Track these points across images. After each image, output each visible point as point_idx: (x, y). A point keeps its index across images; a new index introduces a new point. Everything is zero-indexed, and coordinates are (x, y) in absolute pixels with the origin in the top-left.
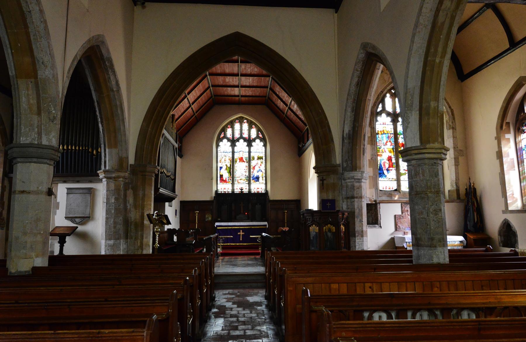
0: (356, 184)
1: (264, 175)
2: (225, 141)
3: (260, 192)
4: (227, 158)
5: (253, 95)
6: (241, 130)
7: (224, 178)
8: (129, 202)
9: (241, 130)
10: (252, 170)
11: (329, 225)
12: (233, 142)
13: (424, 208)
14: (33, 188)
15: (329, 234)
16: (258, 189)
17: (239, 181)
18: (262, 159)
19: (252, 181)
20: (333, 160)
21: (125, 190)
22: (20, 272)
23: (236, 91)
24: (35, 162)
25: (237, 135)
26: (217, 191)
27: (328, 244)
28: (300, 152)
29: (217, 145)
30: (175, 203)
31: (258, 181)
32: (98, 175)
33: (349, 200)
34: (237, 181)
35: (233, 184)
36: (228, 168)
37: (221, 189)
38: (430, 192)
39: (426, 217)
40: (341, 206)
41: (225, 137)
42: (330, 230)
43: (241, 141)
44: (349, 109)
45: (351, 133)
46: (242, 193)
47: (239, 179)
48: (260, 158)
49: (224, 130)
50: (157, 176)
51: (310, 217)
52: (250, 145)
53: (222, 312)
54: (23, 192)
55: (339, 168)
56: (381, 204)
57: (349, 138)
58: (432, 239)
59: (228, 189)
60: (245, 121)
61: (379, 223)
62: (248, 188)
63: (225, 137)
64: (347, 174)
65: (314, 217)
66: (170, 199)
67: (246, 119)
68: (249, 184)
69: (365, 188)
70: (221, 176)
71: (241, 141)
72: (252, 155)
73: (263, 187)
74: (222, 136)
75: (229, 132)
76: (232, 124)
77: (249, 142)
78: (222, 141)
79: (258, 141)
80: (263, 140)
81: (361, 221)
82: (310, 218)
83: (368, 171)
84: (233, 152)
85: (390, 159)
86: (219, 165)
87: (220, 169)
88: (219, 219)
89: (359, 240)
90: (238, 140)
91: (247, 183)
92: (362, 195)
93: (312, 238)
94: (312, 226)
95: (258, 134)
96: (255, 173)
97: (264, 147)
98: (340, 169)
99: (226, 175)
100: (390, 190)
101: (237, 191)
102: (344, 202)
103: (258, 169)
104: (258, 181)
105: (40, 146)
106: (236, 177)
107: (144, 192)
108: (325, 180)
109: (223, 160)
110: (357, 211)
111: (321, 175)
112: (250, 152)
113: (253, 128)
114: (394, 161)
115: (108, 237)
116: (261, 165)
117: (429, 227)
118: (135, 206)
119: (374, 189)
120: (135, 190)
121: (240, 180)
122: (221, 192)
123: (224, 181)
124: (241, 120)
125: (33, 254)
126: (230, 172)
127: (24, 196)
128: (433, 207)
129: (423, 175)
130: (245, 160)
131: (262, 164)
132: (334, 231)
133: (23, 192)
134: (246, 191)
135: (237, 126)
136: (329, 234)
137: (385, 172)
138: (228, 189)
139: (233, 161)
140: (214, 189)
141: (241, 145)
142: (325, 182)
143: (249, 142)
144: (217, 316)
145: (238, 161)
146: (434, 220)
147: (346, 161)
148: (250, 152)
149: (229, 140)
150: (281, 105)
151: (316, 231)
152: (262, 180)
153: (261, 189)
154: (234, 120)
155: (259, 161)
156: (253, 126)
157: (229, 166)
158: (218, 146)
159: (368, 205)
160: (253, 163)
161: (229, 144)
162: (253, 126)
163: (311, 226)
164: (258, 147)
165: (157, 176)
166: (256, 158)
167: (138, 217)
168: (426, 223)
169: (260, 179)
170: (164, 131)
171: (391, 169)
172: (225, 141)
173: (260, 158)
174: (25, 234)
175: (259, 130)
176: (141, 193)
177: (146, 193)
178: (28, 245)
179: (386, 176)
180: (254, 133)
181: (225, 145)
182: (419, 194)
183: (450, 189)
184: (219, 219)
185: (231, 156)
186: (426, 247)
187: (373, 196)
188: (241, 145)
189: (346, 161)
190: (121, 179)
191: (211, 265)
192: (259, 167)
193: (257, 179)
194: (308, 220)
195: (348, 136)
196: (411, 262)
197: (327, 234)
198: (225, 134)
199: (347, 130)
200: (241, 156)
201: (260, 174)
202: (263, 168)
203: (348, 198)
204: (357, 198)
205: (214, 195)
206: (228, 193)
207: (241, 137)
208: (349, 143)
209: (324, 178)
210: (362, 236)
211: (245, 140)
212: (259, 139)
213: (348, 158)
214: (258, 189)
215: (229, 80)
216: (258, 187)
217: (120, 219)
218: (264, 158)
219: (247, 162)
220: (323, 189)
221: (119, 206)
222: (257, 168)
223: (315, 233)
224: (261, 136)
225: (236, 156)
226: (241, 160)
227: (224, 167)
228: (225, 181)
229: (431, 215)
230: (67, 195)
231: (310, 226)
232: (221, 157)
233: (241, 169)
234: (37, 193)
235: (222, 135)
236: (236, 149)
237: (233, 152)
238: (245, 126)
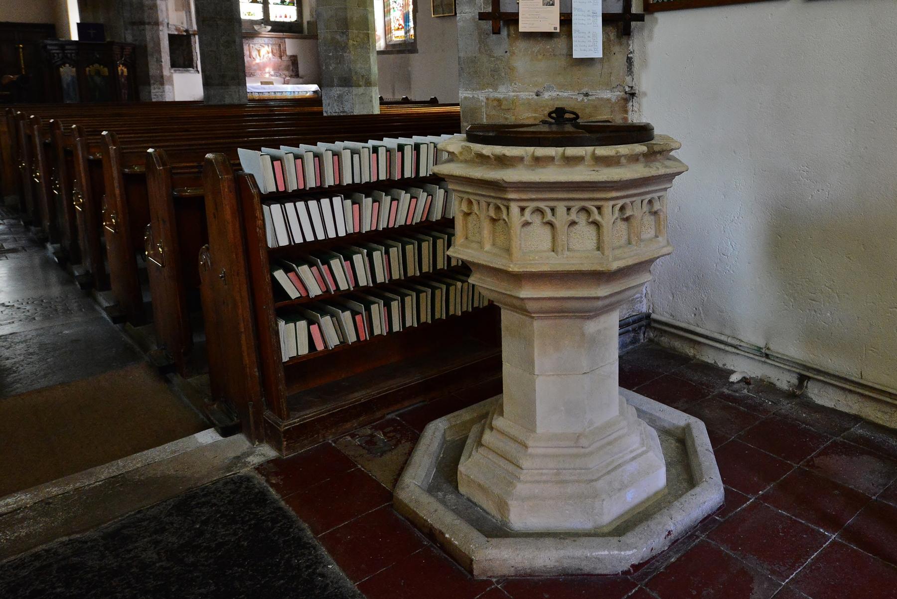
11: (96, 65)
33: (135, 27)
40: (123, 36)
51: (58, 51)
61: (195, 65)
69: (164, 9)
81: (159, 61)
82: (58, 54)
92: (157, 18)
93: (65, 86)
94: (65, 66)
102: (127, 30)
110: (150, 46)
119: (184, 12)
159: (171, 37)
163: (63, 66)
183: (309, 20)
187: (182, 23)
194: (55, 56)
203: (133, 24)
204: (149, 23)
231: (60, 66)
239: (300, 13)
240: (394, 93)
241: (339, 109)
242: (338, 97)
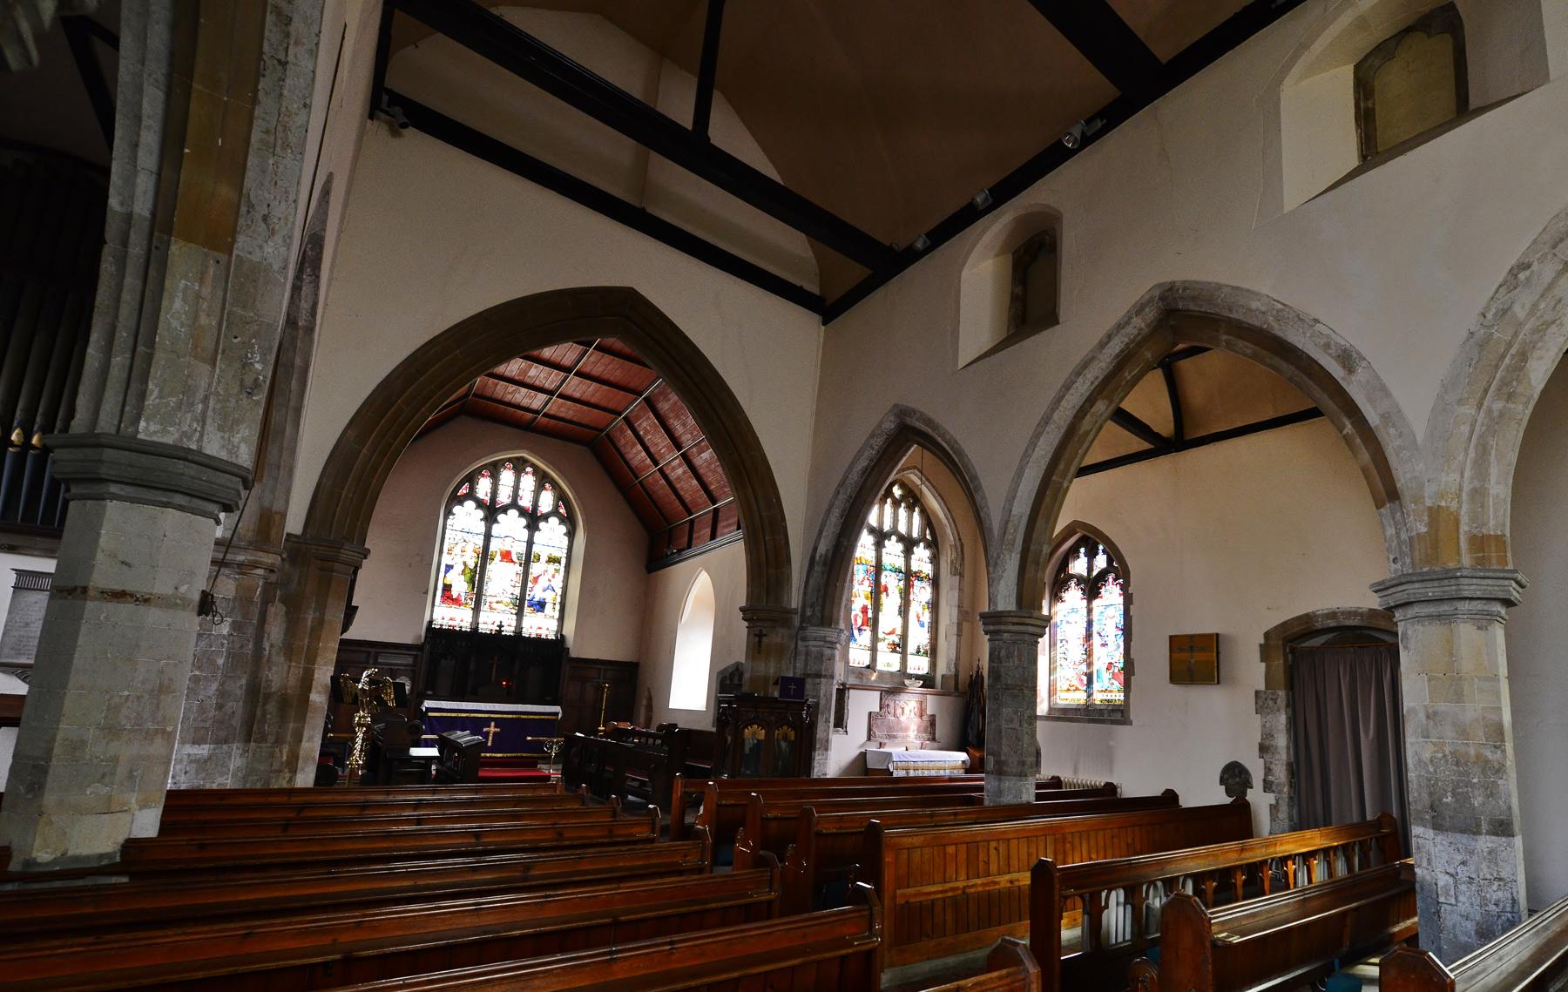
0: (827, 652)
1: (559, 600)
2: (470, 504)
3: (458, 629)
4: (470, 548)
5: (575, 419)
6: (516, 488)
7: (453, 593)
8: (268, 639)
9: (516, 488)
10: (530, 585)
12: (492, 511)
13: (1016, 713)
14: (162, 587)
15: (784, 745)
16: (540, 628)
17: (494, 605)
18: (560, 563)
19: (527, 610)
20: (786, 599)
21: (266, 601)
22: (77, 859)
24: (181, 508)
25: (504, 497)
26: (431, 622)
27: (780, 763)
29: (447, 511)
31: (543, 611)
34: (488, 604)
35: (477, 610)
36: (468, 571)
37: (443, 619)
38: (1027, 687)
39: (1017, 727)
41: (471, 495)
42: (785, 738)
43: (513, 513)
44: (836, 512)
45: (830, 555)
46: (497, 637)
47: (495, 600)
48: (552, 560)
49: (472, 479)
54: (120, 596)
55: (794, 616)
56: (851, 691)
57: (825, 564)
58: (1023, 763)
59: (462, 621)
60: (529, 469)
61: (844, 725)
62: (514, 623)
63: (471, 495)
64: (813, 631)
65: (758, 710)
67: (533, 465)
68: (520, 615)
70: (447, 588)
71: (513, 513)
72: (535, 549)
73: (554, 625)
74: (465, 492)
75: (484, 487)
76: (494, 471)
77: (533, 519)
78: (461, 501)
79: (554, 521)
80: (569, 521)
81: (827, 721)
84: (488, 536)
85: (864, 610)
86: (446, 560)
87: (447, 571)
88: (429, 693)
89: (820, 757)
90: (504, 510)
91: (514, 611)
95: (556, 507)
96: (536, 593)
97: (566, 538)
98: (797, 620)
99: (460, 587)
100: (859, 666)
103: (546, 584)
104: (543, 611)
106: (487, 594)
107: (323, 614)
108: (765, 635)
109: (457, 550)
110: (822, 702)
111: (759, 626)
112: (530, 543)
113: (545, 489)
114: (870, 615)
116: (553, 576)
117: (1020, 743)
118: (289, 650)
120: (294, 608)
121: (497, 602)
122: (442, 625)
123: (453, 599)
124: (519, 466)
125: (133, 799)
126: (472, 581)
127: (125, 609)
128: (1028, 711)
129: (1020, 660)
130: (515, 559)
131: (557, 575)
132: (793, 739)
133: (120, 596)
134: (508, 630)
135: (507, 477)
136: (784, 745)
137: (856, 632)
138: (462, 621)
139: (485, 555)
140: (427, 618)
141: (511, 526)
142: (765, 640)
143: (533, 519)
145: (498, 557)
146: (1027, 733)
147: (812, 606)
148: (530, 543)
149: (480, 504)
150: (637, 456)
151: (760, 738)
152: (552, 611)
153: (548, 629)
154: (501, 460)
155: (552, 567)
156: (547, 485)
157: (472, 565)
158: (449, 513)
160: (535, 569)
161: (480, 514)
162: (547, 485)
164: (553, 535)
166: (544, 558)
167: (293, 681)
168: (1017, 737)
169: (548, 607)
171: (865, 627)
172: (470, 504)
173: (552, 560)
174: (112, 731)
175: (561, 497)
176: (310, 617)
177: (328, 617)
178: (122, 771)
179: (855, 640)
180: (547, 501)
181: (467, 517)
182: (1009, 689)
184: (429, 693)
185: (480, 543)
186: (1014, 776)
188: (511, 526)
189: (812, 606)
190: (260, 572)
192: (550, 581)
193: (540, 606)
195: (823, 558)
196: (980, 801)
197: (779, 745)
198: (472, 489)
200: (507, 548)
202: (558, 583)
204: (825, 676)
206: (461, 630)
207: (514, 504)
208: (823, 573)
209: (764, 632)
210: (827, 749)
211: (523, 512)
212: (559, 519)
213: (817, 600)
214: (540, 628)
216: (540, 625)
217: (239, 685)
218: (563, 561)
219: (520, 565)
220: (759, 652)
221: (241, 647)
222: (543, 582)
223: (755, 741)
224: (562, 511)
225: (495, 546)
226: (506, 556)
227: (459, 568)
228: (457, 602)
229: (1026, 725)
230: (14, 592)
232: (452, 541)
233: (502, 580)
234: (171, 603)
235: (464, 490)
236: (496, 529)
237: (488, 536)
238: (528, 482)
239: (933, 665)
240: (1076, 771)
241: (1492, 875)
242: (1490, 853)
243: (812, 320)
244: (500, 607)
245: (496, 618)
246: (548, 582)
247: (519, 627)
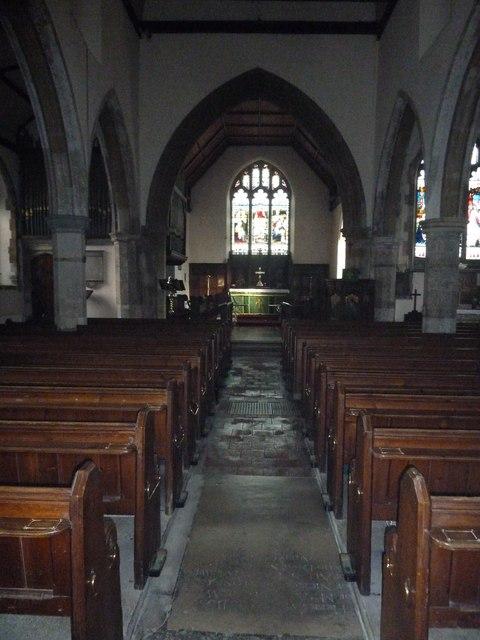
4: (244, 213)
6: (261, 177)
9: (261, 177)
12: (251, 193)
19: (272, 241)
23: (255, 130)
25: (256, 184)
28: (332, 207)
30: (185, 267)
32: (109, 237)
35: (250, 244)
43: (261, 191)
48: (282, 213)
49: (240, 178)
50: (168, 237)
52: (270, 197)
53: (239, 372)
57: (382, 198)
63: (241, 186)
66: (180, 263)
68: (269, 244)
70: (236, 234)
71: (261, 191)
72: (273, 208)
73: (286, 248)
77: (270, 192)
80: (286, 190)
83: (403, 235)
84: (251, 206)
86: (234, 221)
90: (256, 190)
95: (281, 183)
96: (277, 231)
99: (242, 233)
101: (255, 252)
105: (74, 217)
112: (270, 205)
115: (123, 303)
126: (246, 230)
134: (265, 252)
135: (256, 172)
139: (250, 216)
140: (228, 250)
141: (261, 197)
143: (270, 192)
144: (234, 374)
145: (256, 216)
148: (270, 205)
149: (245, 190)
152: (284, 240)
158: (232, 197)
160: (274, 219)
161: (246, 195)
164: (281, 200)
165: (168, 237)
166: (278, 212)
169: (283, 238)
170: (176, 188)
172: (241, 191)
173: (282, 213)
180: (276, 180)
181: (240, 197)
188: (261, 197)
191: (229, 334)
193: (278, 238)
198: (241, 183)
199: (379, 190)
200: (260, 210)
201: (282, 232)
203: (376, 266)
205: (227, 257)
207: (261, 187)
211: (265, 189)
215: (246, 119)
216: (280, 248)
218: (287, 213)
222: (279, 225)
224: (284, 185)
225: (255, 210)
226: (260, 215)
227: (240, 224)
228: (241, 241)
233: (260, 227)
235: (237, 184)
237: (251, 206)
238: (266, 172)
243: (368, 41)
244: (260, 241)
245: (259, 247)
246: (282, 225)
247: (270, 251)
